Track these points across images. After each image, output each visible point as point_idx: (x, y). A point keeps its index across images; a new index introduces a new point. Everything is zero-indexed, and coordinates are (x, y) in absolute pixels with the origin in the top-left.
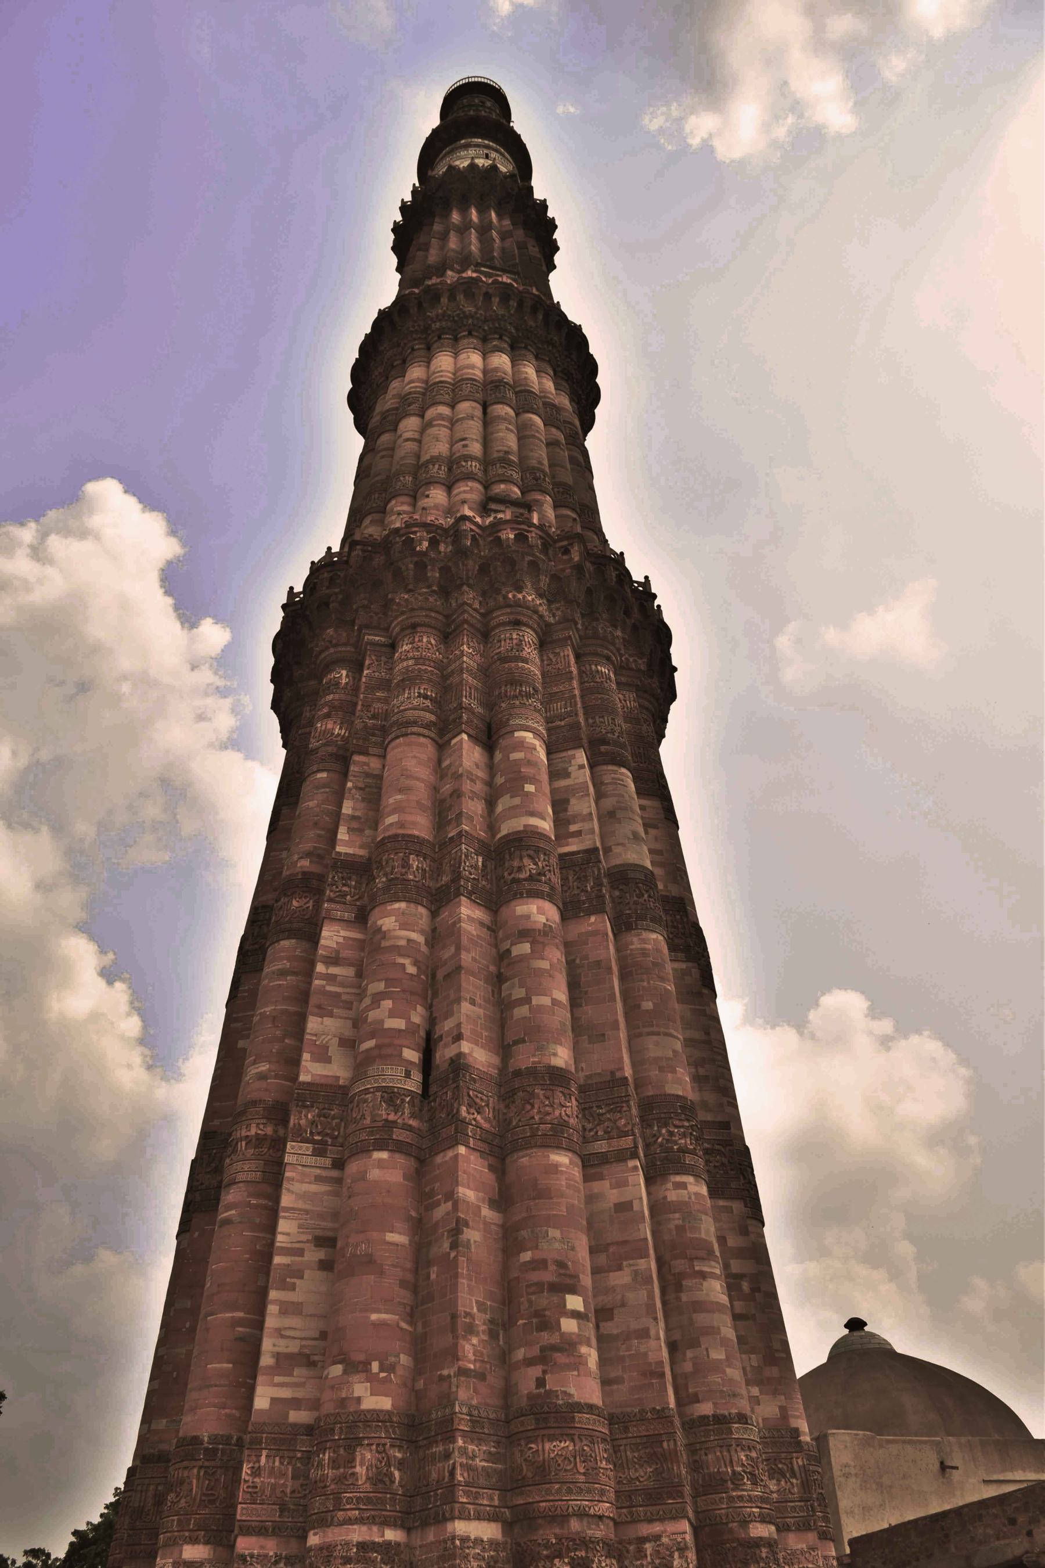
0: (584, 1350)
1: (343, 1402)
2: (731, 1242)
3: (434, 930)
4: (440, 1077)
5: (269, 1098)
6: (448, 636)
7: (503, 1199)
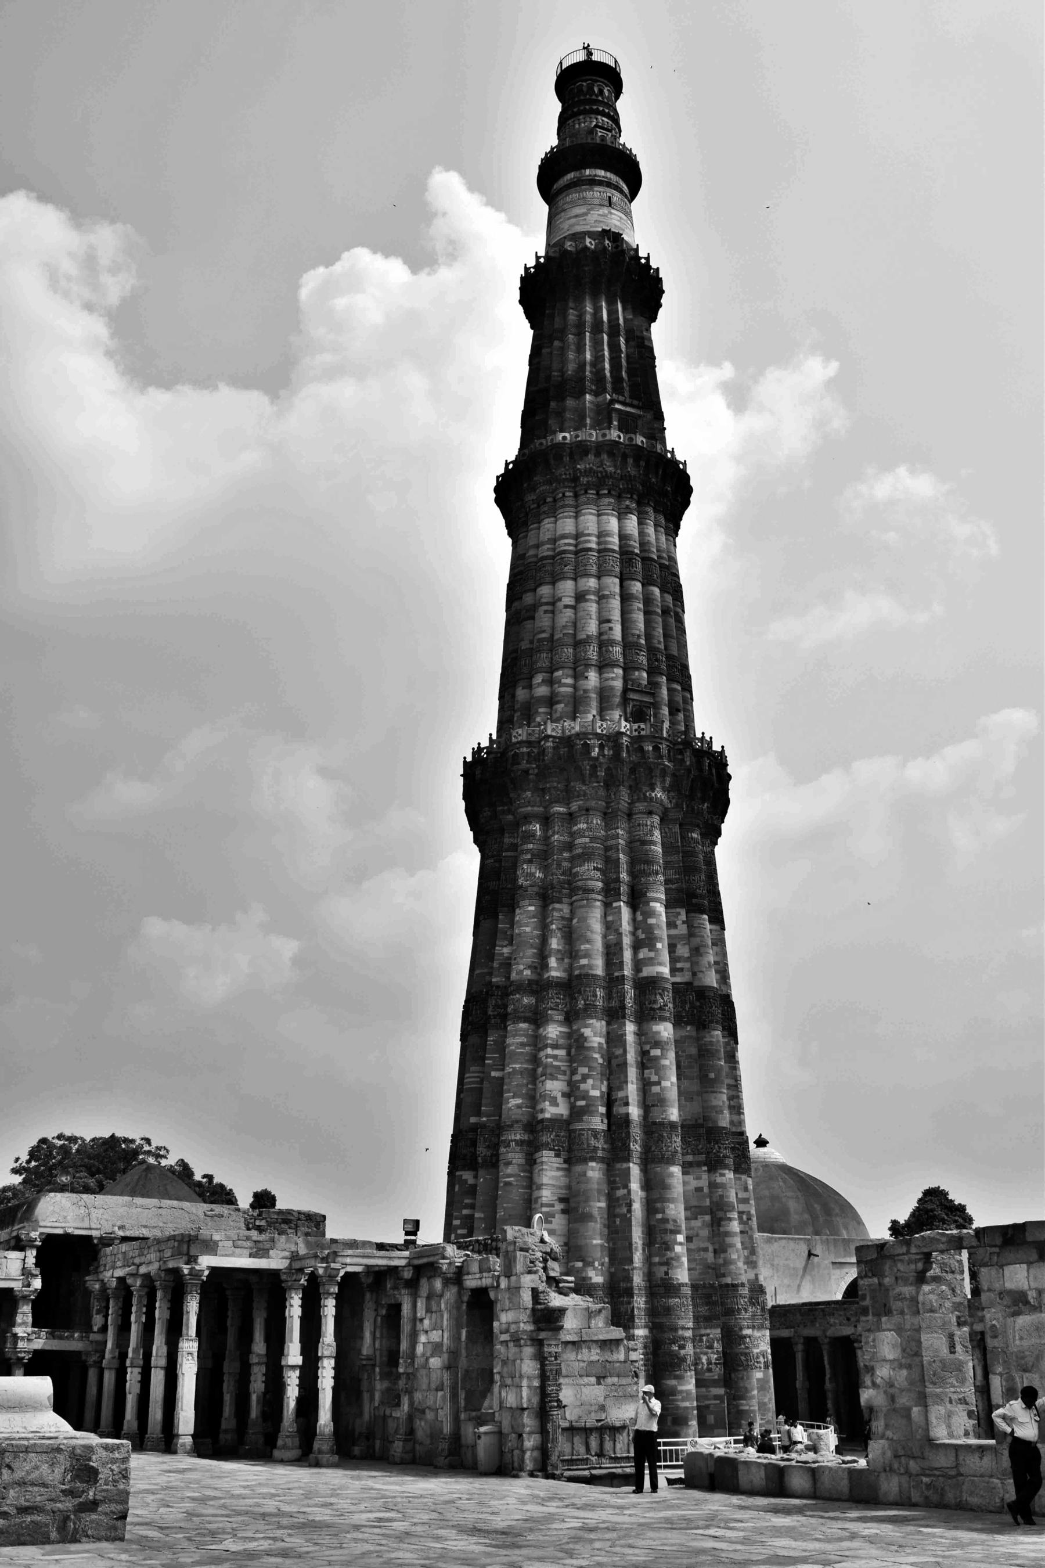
3: (608, 1033)
5: (525, 1121)
6: (609, 817)
7: (648, 1185)
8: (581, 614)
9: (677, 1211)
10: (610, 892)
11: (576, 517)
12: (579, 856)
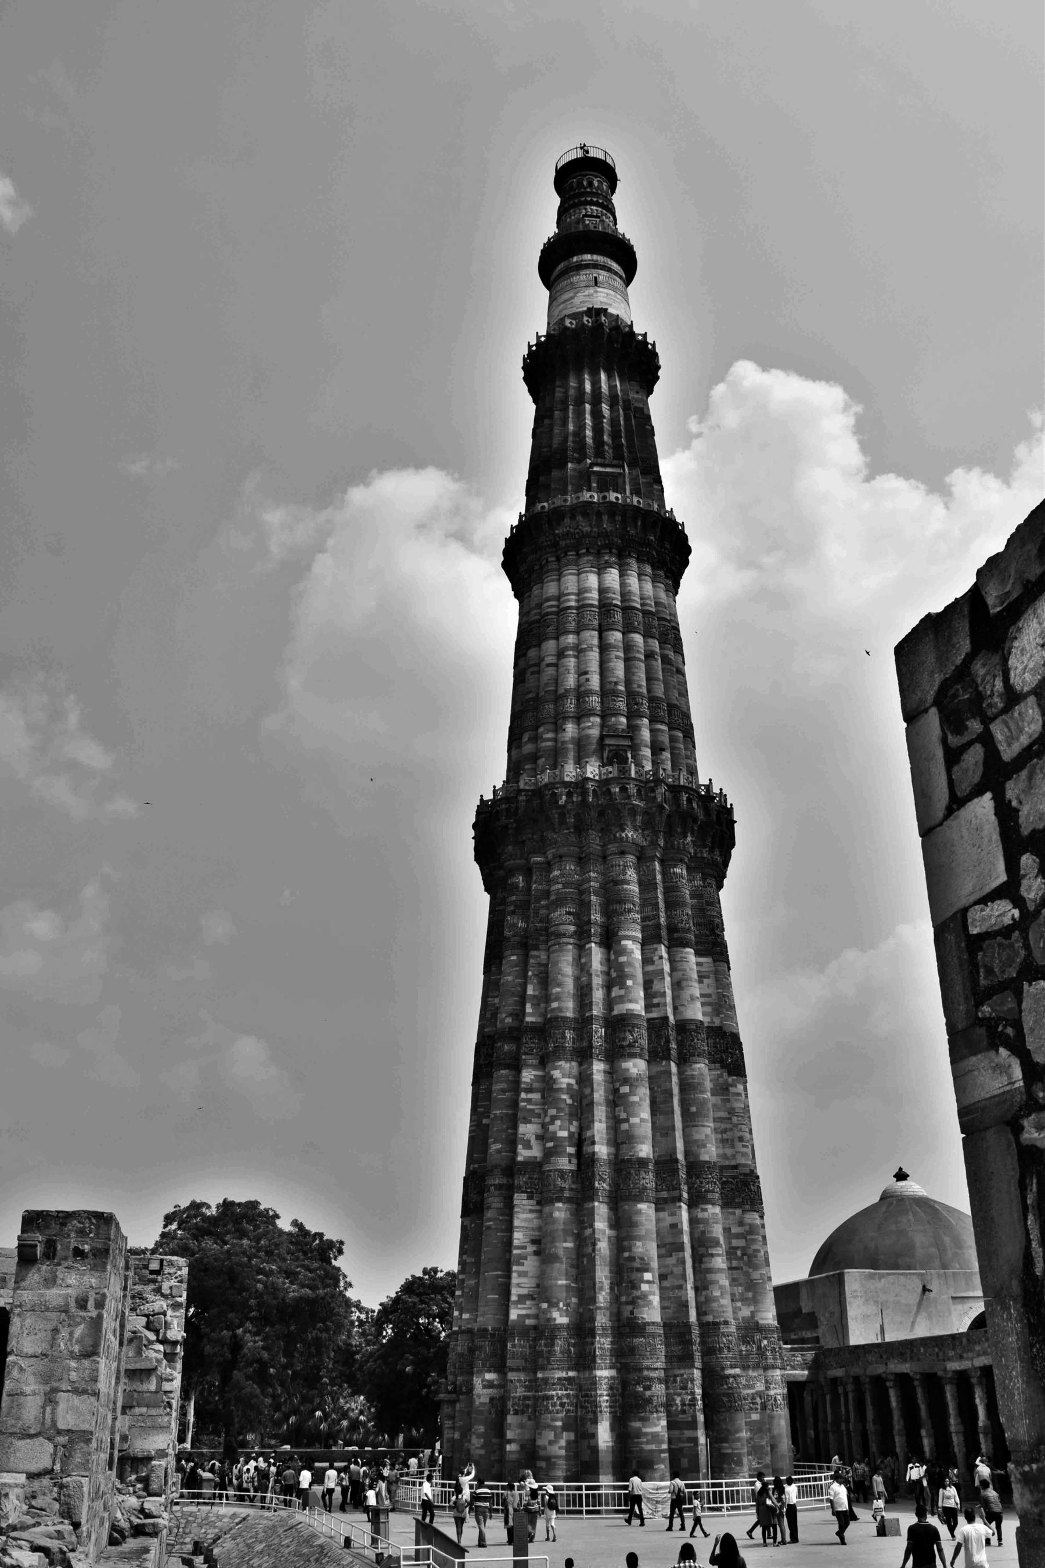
0: (651, 1297)
1: (549, 1320)
2: (733, 1231)
3: (580, 1074)
4: (585, 1161)
6: (582, 861)
8: (561, 670)
9: (647, 1248)
10: (582, 936)
11: (559, 580)
12: (553, 902)
